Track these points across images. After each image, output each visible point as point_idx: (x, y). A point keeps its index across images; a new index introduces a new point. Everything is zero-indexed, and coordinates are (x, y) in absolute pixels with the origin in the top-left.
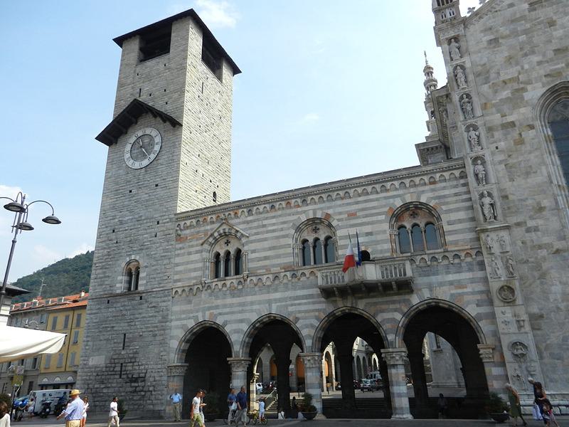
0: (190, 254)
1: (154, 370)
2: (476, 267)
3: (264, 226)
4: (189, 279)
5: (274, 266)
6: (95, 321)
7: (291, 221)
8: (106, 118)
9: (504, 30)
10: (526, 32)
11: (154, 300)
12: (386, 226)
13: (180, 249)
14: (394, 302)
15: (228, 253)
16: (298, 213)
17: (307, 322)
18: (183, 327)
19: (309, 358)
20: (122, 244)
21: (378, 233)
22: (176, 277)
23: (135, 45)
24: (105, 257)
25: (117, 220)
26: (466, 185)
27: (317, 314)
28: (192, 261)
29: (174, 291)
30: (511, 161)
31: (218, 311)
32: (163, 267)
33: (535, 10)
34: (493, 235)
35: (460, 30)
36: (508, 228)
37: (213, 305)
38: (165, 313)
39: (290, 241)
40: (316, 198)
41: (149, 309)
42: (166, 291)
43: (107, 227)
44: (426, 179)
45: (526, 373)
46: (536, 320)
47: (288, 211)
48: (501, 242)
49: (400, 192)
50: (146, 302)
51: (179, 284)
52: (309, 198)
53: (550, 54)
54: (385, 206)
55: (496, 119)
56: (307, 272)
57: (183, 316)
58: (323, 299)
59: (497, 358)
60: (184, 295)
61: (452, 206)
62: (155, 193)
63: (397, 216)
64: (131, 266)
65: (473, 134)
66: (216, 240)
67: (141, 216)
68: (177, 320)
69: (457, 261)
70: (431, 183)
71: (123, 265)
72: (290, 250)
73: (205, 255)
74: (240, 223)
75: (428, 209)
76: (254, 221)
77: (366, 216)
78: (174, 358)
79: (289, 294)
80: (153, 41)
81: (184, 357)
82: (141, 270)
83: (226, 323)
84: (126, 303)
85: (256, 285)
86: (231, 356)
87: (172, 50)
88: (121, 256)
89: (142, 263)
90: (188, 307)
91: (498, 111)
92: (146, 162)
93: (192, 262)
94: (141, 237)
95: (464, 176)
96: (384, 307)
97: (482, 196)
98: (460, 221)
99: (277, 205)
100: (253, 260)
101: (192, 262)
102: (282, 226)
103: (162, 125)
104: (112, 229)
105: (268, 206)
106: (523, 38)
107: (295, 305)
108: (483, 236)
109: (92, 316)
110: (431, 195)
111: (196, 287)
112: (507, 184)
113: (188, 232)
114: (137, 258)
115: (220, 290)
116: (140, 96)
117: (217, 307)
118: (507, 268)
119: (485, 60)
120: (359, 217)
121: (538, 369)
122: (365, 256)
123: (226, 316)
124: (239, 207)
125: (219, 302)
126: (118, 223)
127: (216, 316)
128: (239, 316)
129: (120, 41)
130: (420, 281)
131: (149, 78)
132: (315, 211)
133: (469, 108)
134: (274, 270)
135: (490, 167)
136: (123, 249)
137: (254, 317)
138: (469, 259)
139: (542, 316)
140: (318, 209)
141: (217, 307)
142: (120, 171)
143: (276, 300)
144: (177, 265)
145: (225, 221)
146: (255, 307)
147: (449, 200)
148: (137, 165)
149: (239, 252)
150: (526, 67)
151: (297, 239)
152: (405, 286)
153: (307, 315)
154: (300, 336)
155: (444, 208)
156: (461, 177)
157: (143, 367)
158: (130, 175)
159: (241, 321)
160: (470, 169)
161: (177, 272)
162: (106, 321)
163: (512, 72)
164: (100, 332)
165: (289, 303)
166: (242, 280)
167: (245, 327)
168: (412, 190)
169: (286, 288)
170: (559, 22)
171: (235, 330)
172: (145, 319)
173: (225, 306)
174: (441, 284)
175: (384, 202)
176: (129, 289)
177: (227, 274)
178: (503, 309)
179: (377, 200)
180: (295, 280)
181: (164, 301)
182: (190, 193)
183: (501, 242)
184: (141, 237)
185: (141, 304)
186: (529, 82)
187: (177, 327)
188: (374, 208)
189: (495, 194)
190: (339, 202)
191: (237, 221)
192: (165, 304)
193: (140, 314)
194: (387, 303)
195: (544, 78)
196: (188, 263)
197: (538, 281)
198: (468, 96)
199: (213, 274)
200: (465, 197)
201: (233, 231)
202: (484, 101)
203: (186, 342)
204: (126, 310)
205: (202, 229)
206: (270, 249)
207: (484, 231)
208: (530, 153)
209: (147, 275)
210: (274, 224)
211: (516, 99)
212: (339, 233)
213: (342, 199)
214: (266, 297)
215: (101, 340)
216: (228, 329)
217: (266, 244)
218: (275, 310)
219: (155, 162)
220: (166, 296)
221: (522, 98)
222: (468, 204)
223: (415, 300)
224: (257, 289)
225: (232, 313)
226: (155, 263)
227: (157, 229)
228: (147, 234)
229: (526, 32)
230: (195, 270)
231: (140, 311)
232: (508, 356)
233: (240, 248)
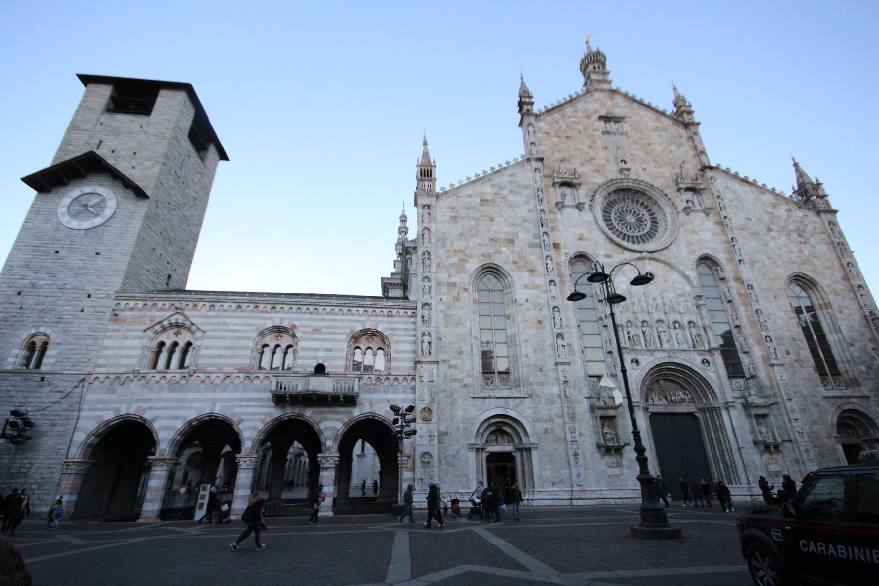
1: (43, 466)
2: (409, 391)
3: (225, 324)
4: (119, 366)
5: (227, 365)
7: (254, 325)
8: (43, 162)
9: (462, 213)
10: (475, 219)
11: (61, 384)
12: (345, 345)
13: (114, 331)
14: (337, 413)
16: (264, 318)
17: (252, 424)
18: (95, 418)
19: (245, 459)
20: (27, 311)
21: (337, 350)
22: (100, 361)
23: (105, 92)
25: (27, 281)
26: (414, 323)
27: (263, 417)
29: (94, 376)
30: (448, 312)
31: (149, 405)
32: (85, 348)
33: (483, 205)
34: (426, 367)
35: (431, 201)
36: (437, 362)
39: (250, 344)
40: (286, 307)
44: (386, 311)
45: (428, 476)
46: (443, 434)
47: (255, 314)
48: (431, 374)
49: (363, 318)
50: (49, 384)
51: (103, 370)
52: (280, 306)
53: (487, 241)
54: (347, 328)
55: (444, 277)
56: (262, 376)
57: (99, 406)
58: (273, 404)
59: (410, 465)
60: (107, 382)
61: (400, 339)
63: (356, 338)
64: (35, 339)
65: (427, 284)
66: (164, 329)
67: (65, 284)
68: (89, 409)
69: (396, 383)
70: (388, 316)
72: (249, 352)
73: (146, 342)
74: (198, 317)
75: (382, 337)
76: (215, 317)
77: (330, 333)
78: (76, 453)
79: (239, 395)
80: (133, 96)
81: (89, 453)
82: (50, 346)
83: (155, 419)
85: (202, 382)
86: (154, 454)
87: (154, 114)
89: (54, 338)
90: (114, 397)
91: (447, 272)
92: (87, 224)
93: (127, 348)
95: (414, 316)
96: (329, 416)
97: (424, 334)
98: (404, 351)
99: (244, 306)
100: (204, 356)
101: (127, 348)
102: (243, 328)
103: (121, 190)
104: (18, 290)
105: (234, 305)
106: (472, 223)
107: (241, 406)
108: (419, 366)
110: (386, 325)
111: (125, 376)
112: (442, 329)
113: (128, 313)
114: (48, 332)
115: (157, 382)
116: (98, 148)
117: (149, 400)
118: (431, 394)
119: (445, 230)
120: (323, 333)
121: (436, 473)
122: (320, 370)
124: (201, 300)
125: (152, 395)
126: (29, 285)
127: (145, 410)
128: (175, 413)
129: (86, 80)
130: (363, 397)
131: (116, 132)
132: (282, 320)
133: (428, 263)
134: (226, 369)
135: (433, 313)
137: (192, 415)
138: (405, 383)
139: (447, 433)
141: (148, 400)
142: (48, 226)
143: (221, 400)
144: (105, 348)
145: (178, 311)
146: (196, 405)
147: (400, 332)
148: (75, 224)
149: (189, 344)
150: (471, 244)
151: (258, 343)
152: (350, 400)
153: (253, 417)
154: (241, 437)
155: (394, 338)
156: (412, 317)
157: (27, 461)
158: (61, 235)
159: (176, 418)
160: (419, 311)
163: (459, 245)
165: (237, 404)
166: (187, 375)
167: (179, 425)
168: (372, 318)
169: (236, 388)
170: (496, 220)
173: (159, 400)
174: (380, 401)
175: (347, 324)
176: (27, 365)
177: (168, 365)
178: (421, 425)
179: (342, 321)
180: (247, 382)
182: (140, 271)
183: (431, 374)
184: (60, 308)
185: (41, 386)
186: (470, 256)
187: (88, 418)
188: (337, 327)
189: (433, 334)
190: (307, 316)
191: (195, 313)
193: (37, 397)
194: (332, 412)
195: (480, 258)
196: (120, 348)
197: (449, 407)
198: (429, 253)
199: (151, 364)
200: (412, 332)
201: (188, 323)
202: (439, 261)
203: (97, 436)
204: (17, 391)
205: (149, 314)
206: (227, 348)
207: (419, 362)
208: (462, 308)
210: (236, 324)
211: (460, 266)
212: (301, 344)
213: (311, 313)
214: (211, 395)
216: (156, 425)
217: (223, 343)
218: (219, 410)
219: (102, 227)
221: (464, 267)
222: (413, 339)
223: (357, 412)
224: (202, 386)
225: (166, 408)
226: (72, 341)
227: (86, 303)
229: (475, 219)
230: (128, 357)
231: (38, 394)
232: (418, 464)
233: (192, 341)
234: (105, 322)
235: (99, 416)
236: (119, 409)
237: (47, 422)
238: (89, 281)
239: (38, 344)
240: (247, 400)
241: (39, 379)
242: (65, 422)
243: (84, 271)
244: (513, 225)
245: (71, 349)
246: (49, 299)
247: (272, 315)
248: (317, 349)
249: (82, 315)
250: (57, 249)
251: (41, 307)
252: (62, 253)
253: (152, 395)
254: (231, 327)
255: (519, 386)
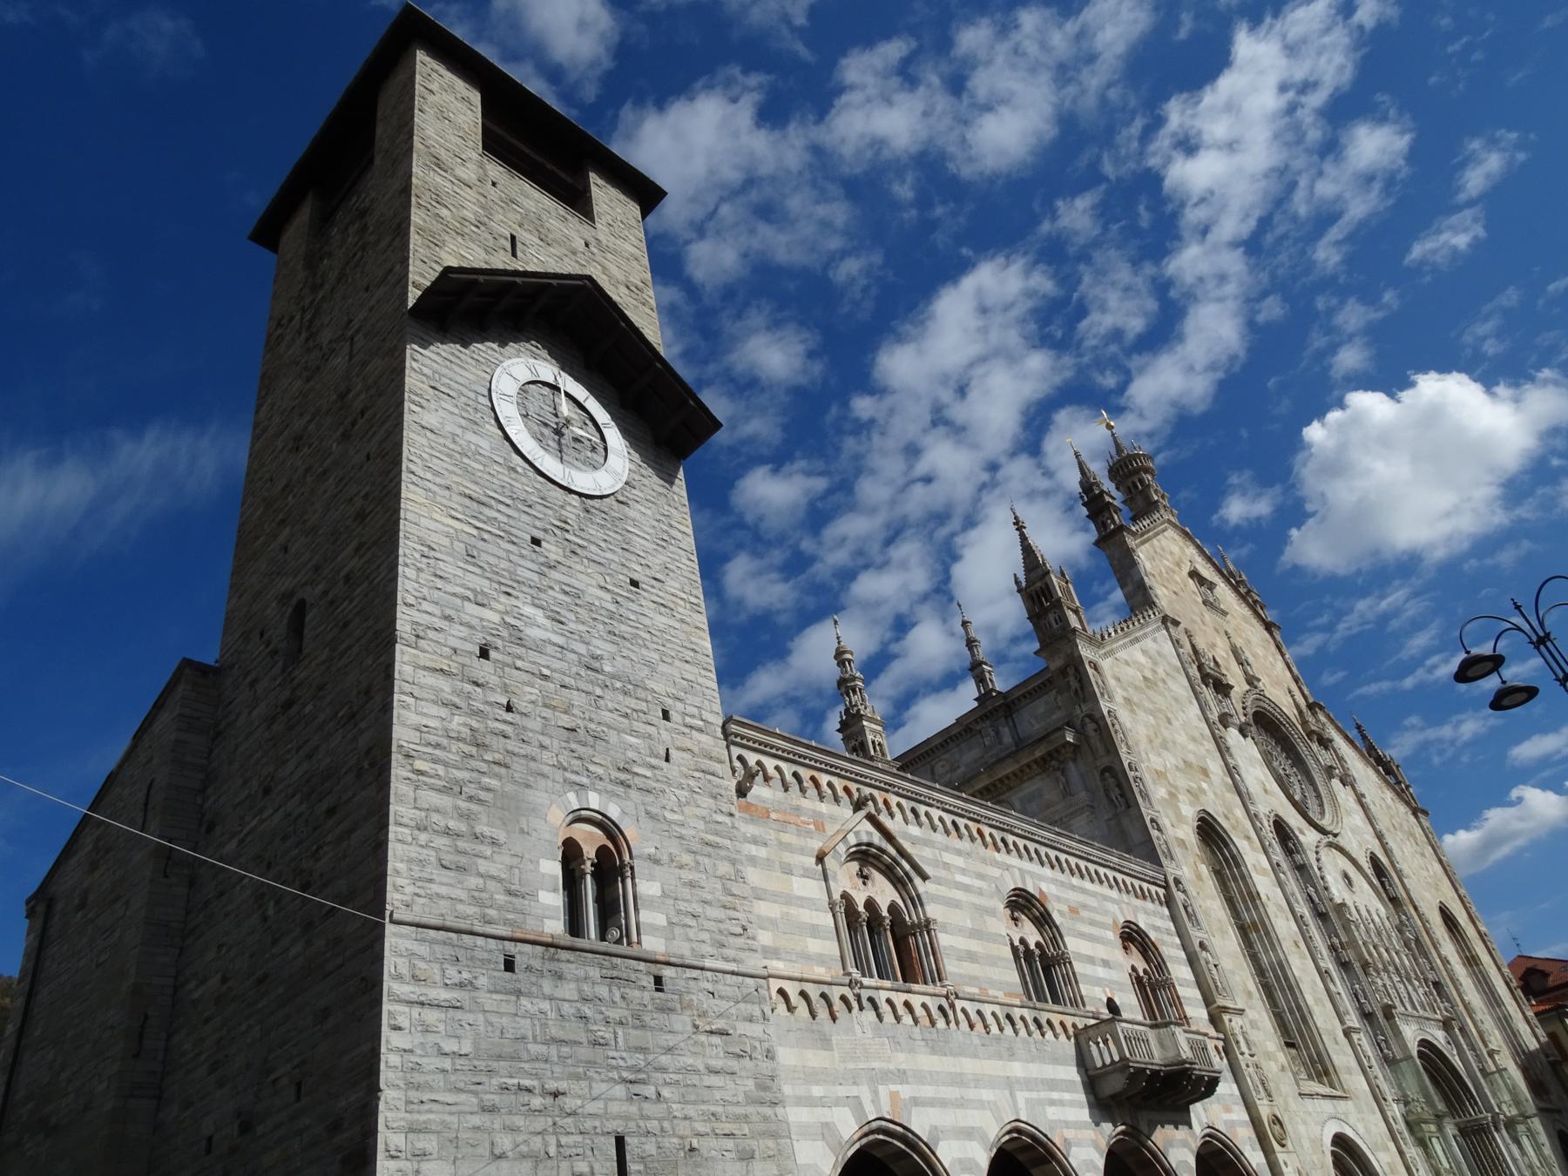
0: (787, 870)
3: (947, 866)
4: (806, 957)
5: (992, 983)
6: (450, 1046)
10: (1152, 713)
13: (755, 841)
15: (870, 904)
16: (996, 864)
18: (826, 1131)
22: (765, 938)
24: (467, 749)
28: (802, 898)
29: (775, 985)
32: (719, 886)
37: (892, 1067)
38: (765, 1066)
41: (703, 1038)
42: (748, 980)
43: (448, 618)
51: (778, 966)
57: (817, 1091)
62: (637, 608)
71: (557, 816)
77: (1092, 923)
84: (603, 991)
88: (544, 776)
94: (613, 737)
101: (802, 902)
102: (977, 883)
104: (480, 638)
105: (948, 818)
109: (431, 1016)
114: (614, 812)
117: (901, 1076)
120: (1082, 921)
123: (931, 1110)
125: (901, 1060)
136: (542, 747)
140: (1029, 872)
141: (901, 1076)
144: (759, 895)
146: (986, 1095)
159: (968, 1133)
161: (759, 917)
162: (515, 1058)
164: (491, 1110)
165: (1044, 1095)
171: (960, 1161)
172: (695, 1079)
173: (921, 1077)
181: (750, 1020)
185: (666, 1010)
190: (1047, 871)
192: (755, 1030)
209: (665, 895)
212: (1073, 945)
215: (501, 1157)
220: (746, 999)
225: (942, 1103)
227: (665, 735)
228: (633, 733)
230: (815, 931)
231: (671, 1040)
234: (734, 810)
235: (826, 1125)
236: (856, 1104)
237: (730, 1144)
238: (649, 664)
239: (589, 852)
240: (1052, 1085)
241: (649, 982)
242: (771, 1143)
243: (623, 627)
244: (1194, 739)
245: (692, 884)
246: (578, 699)
247: (1001, 857)
248: (1091, 960)
249: (670, 770)
250: (539, 535)
251: (566, 721)
252: (551, 549)
253: (901, 1060)
254: (959, 878)
255: (1327, 1073)
